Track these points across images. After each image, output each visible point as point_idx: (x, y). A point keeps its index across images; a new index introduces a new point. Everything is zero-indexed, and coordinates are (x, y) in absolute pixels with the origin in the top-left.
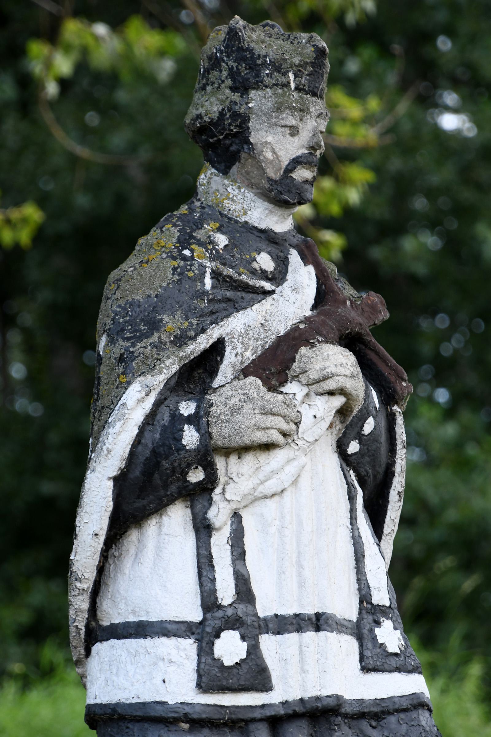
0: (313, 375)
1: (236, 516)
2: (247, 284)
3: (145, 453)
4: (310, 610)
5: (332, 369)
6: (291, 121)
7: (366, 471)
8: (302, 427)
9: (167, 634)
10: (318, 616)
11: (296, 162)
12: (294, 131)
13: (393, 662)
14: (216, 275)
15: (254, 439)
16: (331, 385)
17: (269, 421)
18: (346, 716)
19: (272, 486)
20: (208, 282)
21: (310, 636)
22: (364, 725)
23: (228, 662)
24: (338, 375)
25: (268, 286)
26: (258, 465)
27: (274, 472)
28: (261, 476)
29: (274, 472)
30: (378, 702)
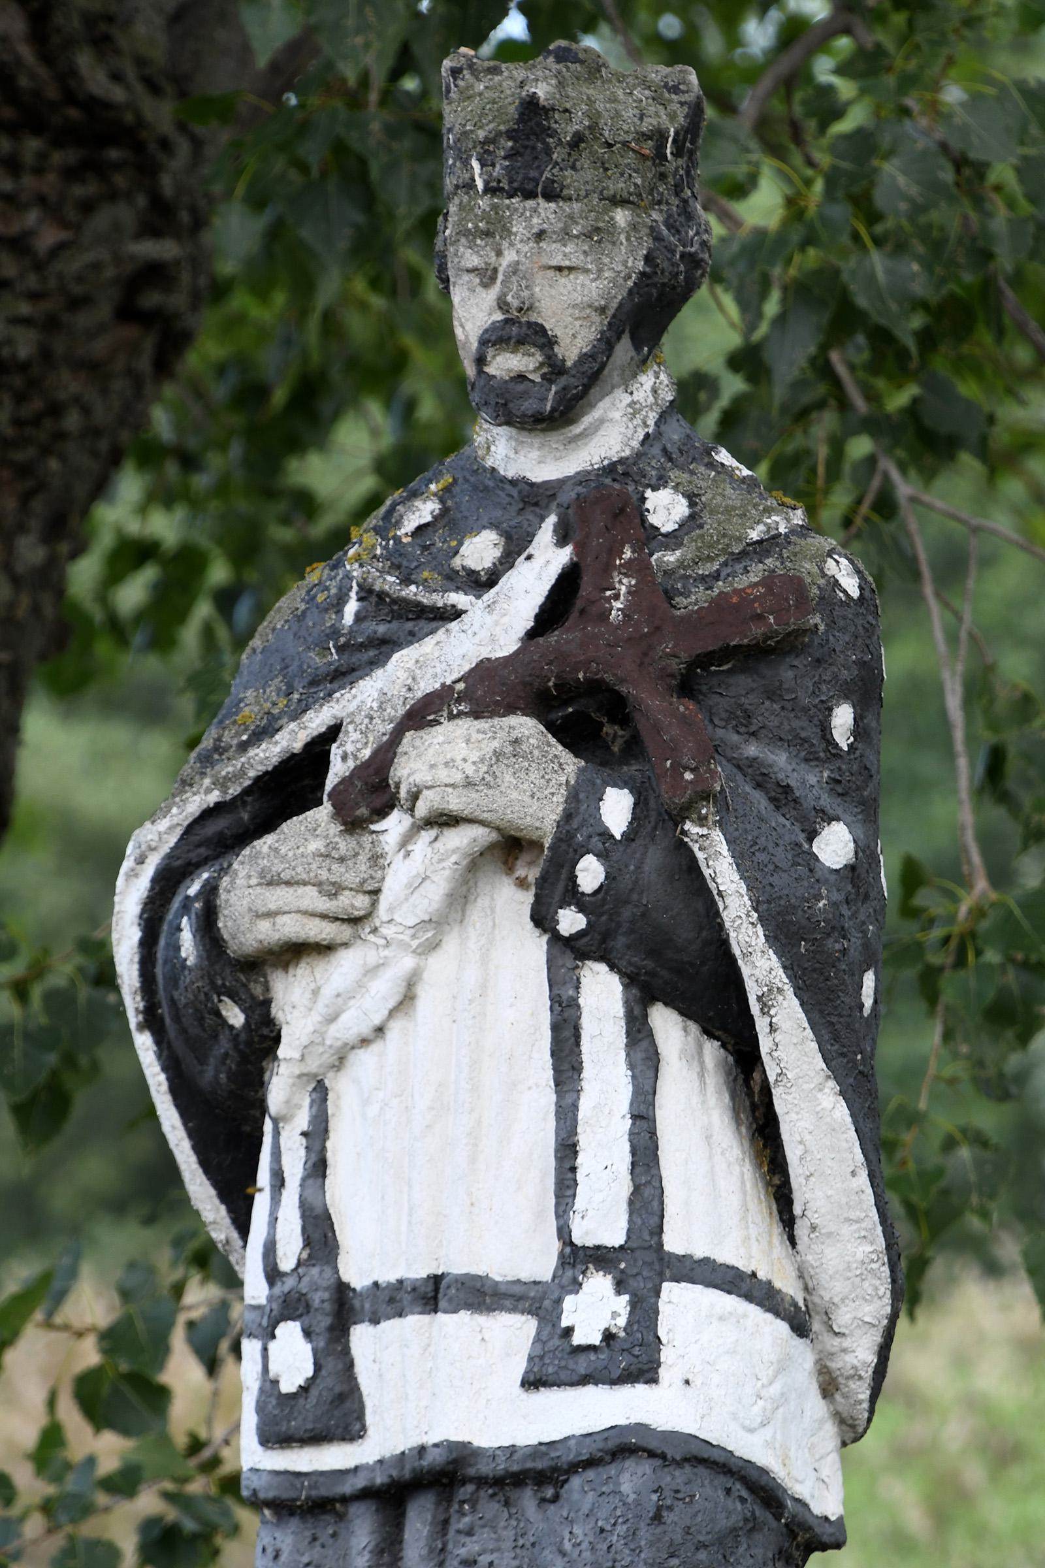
1: (321, 1091)
2: (419, 604)
4: (419, 1271)
7: (630, 963)
10: (436, 1280)
13: (582, 1365)
14: (366, 593)
15: (261, 937)
18: (482, 1481)
19: (352, 1024)
20: (352, 608)
21: (414, 1321)
22: (527, 1499)
24: (428, 788)
25: (458, 599)
26: (313, 986)
27: (344, 998)
28: (321, 1007)
29: (344, 998)
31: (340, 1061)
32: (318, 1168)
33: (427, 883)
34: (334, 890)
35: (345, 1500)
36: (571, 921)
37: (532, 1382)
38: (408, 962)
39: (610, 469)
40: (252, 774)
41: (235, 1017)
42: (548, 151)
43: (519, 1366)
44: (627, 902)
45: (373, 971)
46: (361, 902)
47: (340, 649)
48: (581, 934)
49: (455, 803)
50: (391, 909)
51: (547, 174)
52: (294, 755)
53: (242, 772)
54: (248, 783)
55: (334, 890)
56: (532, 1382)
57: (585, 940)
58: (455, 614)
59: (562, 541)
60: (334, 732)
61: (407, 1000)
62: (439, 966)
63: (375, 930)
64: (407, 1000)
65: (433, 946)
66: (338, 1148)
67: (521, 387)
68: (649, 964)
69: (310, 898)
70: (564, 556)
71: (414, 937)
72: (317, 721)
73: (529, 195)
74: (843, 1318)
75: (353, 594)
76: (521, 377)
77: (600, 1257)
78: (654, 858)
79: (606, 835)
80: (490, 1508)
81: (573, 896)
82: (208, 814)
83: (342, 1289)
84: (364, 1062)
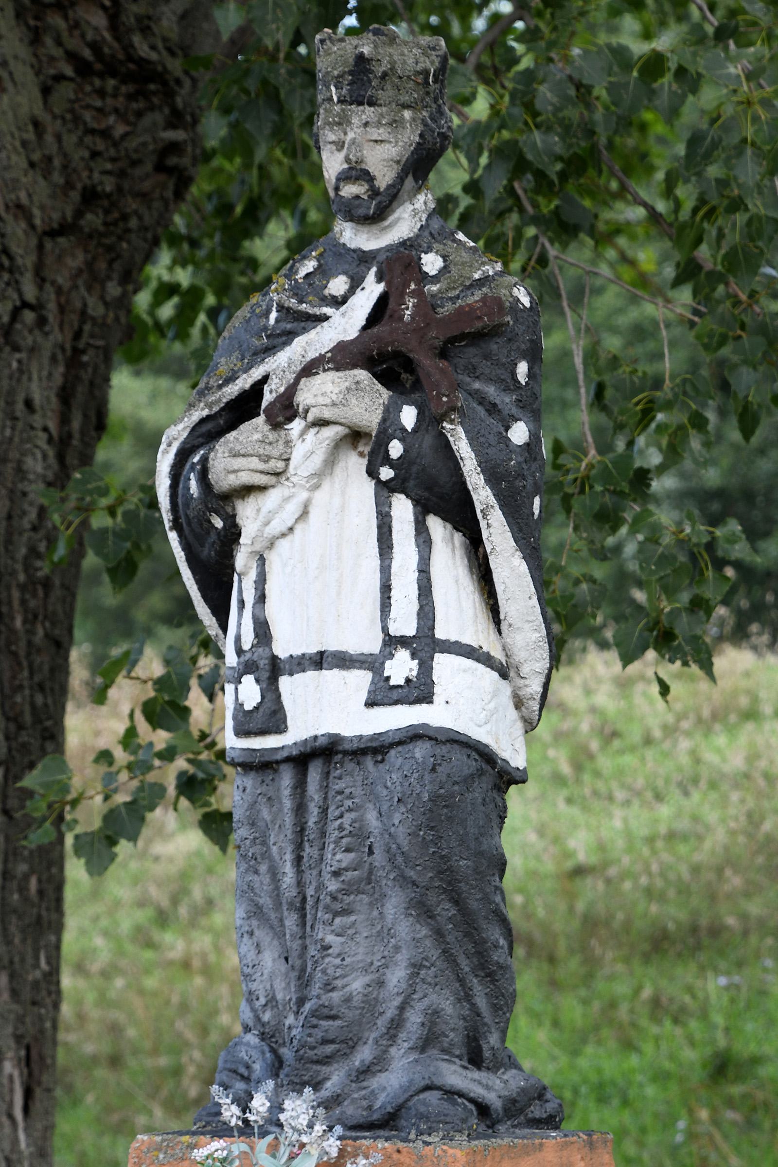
1: (262, 560)
2: (307, 313)
4: (313, 650)
8: (292, 464)
10: (321, 654)
13: (395, 695)
14: (281, 308)
15: (231, 483)
18: (345, 753)
19: (277, 526)
20: (273, 315)
21: (311, 674)
22: (369, 761)
25: (327, 310)
26: (257, 507)
27: (273, 513)
28: (261, 518)
29: (273, 513)
31: (271, 545)
32: (261, 598)
33: (313, 455)
34: (267, 459)
35: (278, 762)
36: (386, 473)
37: (370, 704)
38: (304, 495)
39: (403, 243)
40: (224, 400)
41: (218, 523)
42: (370, 81)
43: (364, 696)
44: (415, 463)
45: (287, 499)
46: (280, 465)
47: (268, 337)
48: (391, 480)
49: (327, 414)
50: (296, 468)
51: (369, 93)
52: (245, 391)
53: (220, 400)
54: (222, 405)
55: (267, 459)
56: (370, 704)
57: (393, 483)
58: (326, 318)
59: (379, 279)
60: (265, 379)
61: (304, 514)
62: (320, 497)
63: (288, 479)
64: (304, 514)
65: (317, 487)
66: (271, 588)
67: (357, 202)
68: (426, 494)
69: (255, 463)
70: (380, 288)
71: (307, 482)
72: (257, 373)
73: (361, 104)
74: (525, 670)
75: (274, 309)
76: (357, 197)
77: (403, 641)
78: (428, 441)
79: (404, 429)
80: (350, 766)
81: (387, 461)
82: (203, 421)
83: (274, 659)
84: (283, 545)
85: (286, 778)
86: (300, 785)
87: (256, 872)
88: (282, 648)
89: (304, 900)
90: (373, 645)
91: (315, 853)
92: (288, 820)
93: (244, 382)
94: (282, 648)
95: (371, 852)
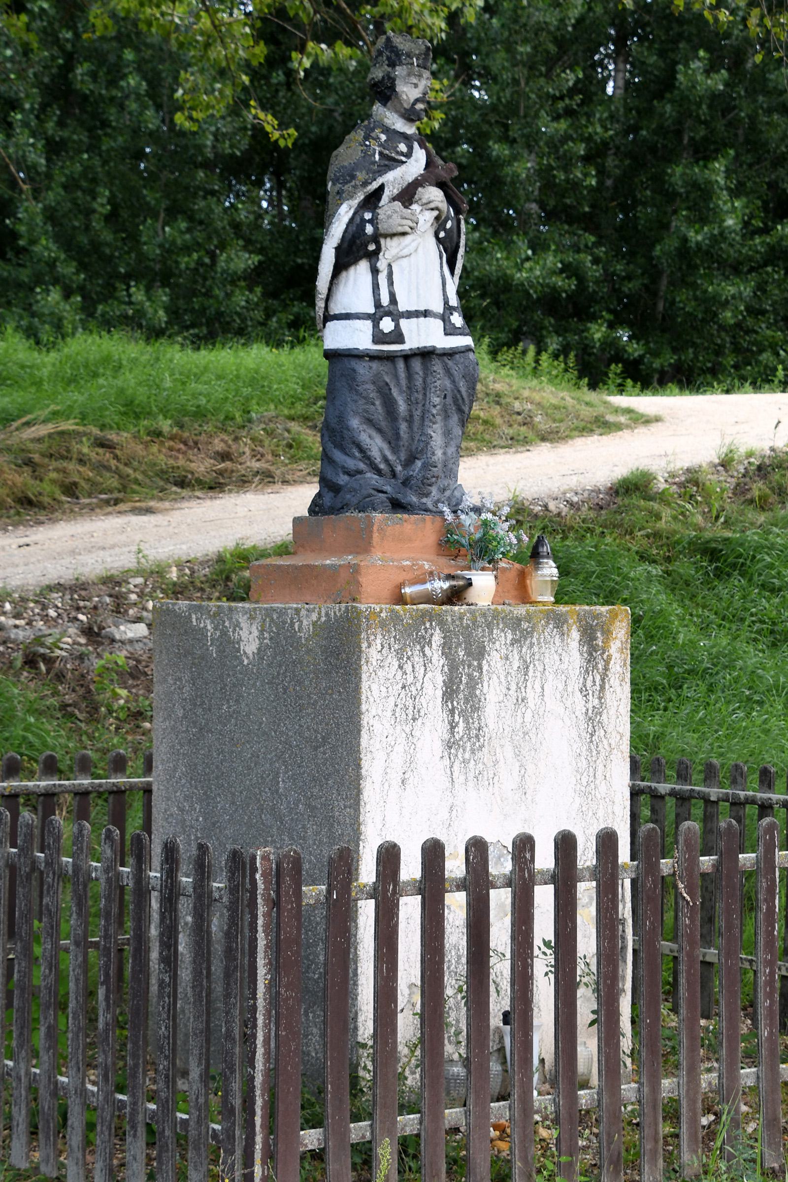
0: (424, 201)
1: (390, 266)
3: (349, 236)
4: (422, 309)
5: (432, 198)
6: (415, 81)
9: (359, 318)
11: (417, 101)
12: (416, 86)
13: (458, 331)
14: (381, 153)
16: (432, 205)
17: (405, 222)
19: (405, 252)
20: (377, 157)
21: (422, 319)
23: (386, 331)
25: (404, 159)
27: (407, 246)
29: (407, 246)
30: (451, 349)
32: (391, 283)
81: (445, 230)
85: (401, 365)
86: (408, 367)
87: (373, 404)
88: (402, 307)
89: (411, 416)
90: (439, 308)
91: (420, 397)
92: (404, 382)
93: (375, 185)
94: (402, 307)
95: (445, 397)
